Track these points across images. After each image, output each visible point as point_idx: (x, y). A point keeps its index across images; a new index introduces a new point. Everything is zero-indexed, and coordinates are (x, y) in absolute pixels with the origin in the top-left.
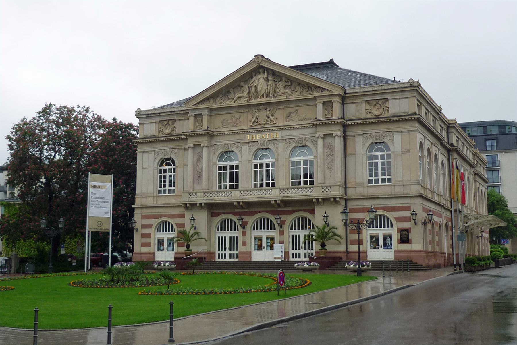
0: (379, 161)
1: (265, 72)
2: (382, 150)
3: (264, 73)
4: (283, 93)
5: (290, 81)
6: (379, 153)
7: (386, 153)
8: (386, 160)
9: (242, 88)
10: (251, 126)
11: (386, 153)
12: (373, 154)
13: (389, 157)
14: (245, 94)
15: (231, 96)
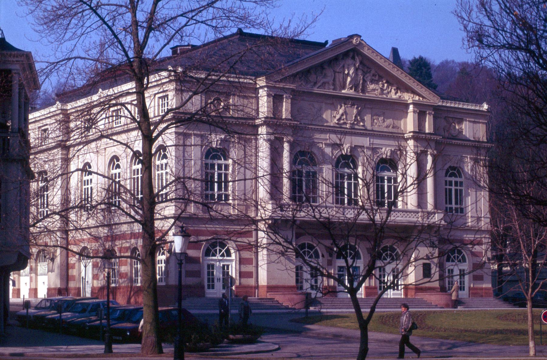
0: (453, 188)
1: (356, 57)
2: (456, 177)
3: (353, 58)
4: (374, 90)
5: (379, 76)
6: (453, 179)
7: (458, 179)
8: (459, 188)
9: (324, 71)
10: (338, 124)
11: (458, 179)
12: (449, 179)
13: (461, 183)
14: (330, 79)
15: (312, 78)
